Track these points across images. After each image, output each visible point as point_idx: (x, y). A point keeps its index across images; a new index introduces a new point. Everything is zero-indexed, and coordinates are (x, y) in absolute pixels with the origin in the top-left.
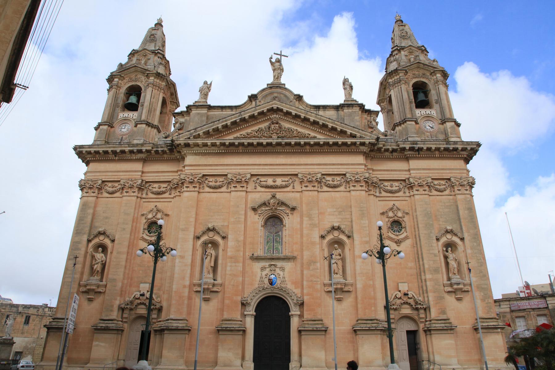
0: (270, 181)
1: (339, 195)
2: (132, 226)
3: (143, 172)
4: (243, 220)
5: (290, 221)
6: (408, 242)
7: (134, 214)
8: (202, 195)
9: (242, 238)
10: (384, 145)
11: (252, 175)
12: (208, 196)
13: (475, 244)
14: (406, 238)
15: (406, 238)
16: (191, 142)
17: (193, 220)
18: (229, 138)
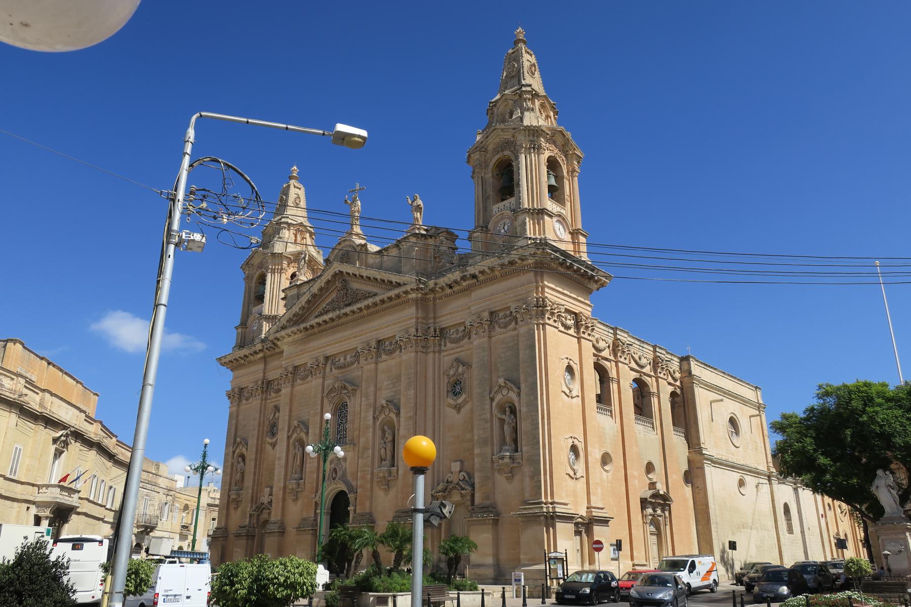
2: (259, 431)
3: (264, 373)
4: (319, 410)
6: (468, 407)
7: (260, 418)
9: (318, 432)
11: (327, 358)
12: (300, 387)
13: (532, 398)
14: (465, 402)
15: (465, 402)
16: (278, 335)
17: (287, 418)
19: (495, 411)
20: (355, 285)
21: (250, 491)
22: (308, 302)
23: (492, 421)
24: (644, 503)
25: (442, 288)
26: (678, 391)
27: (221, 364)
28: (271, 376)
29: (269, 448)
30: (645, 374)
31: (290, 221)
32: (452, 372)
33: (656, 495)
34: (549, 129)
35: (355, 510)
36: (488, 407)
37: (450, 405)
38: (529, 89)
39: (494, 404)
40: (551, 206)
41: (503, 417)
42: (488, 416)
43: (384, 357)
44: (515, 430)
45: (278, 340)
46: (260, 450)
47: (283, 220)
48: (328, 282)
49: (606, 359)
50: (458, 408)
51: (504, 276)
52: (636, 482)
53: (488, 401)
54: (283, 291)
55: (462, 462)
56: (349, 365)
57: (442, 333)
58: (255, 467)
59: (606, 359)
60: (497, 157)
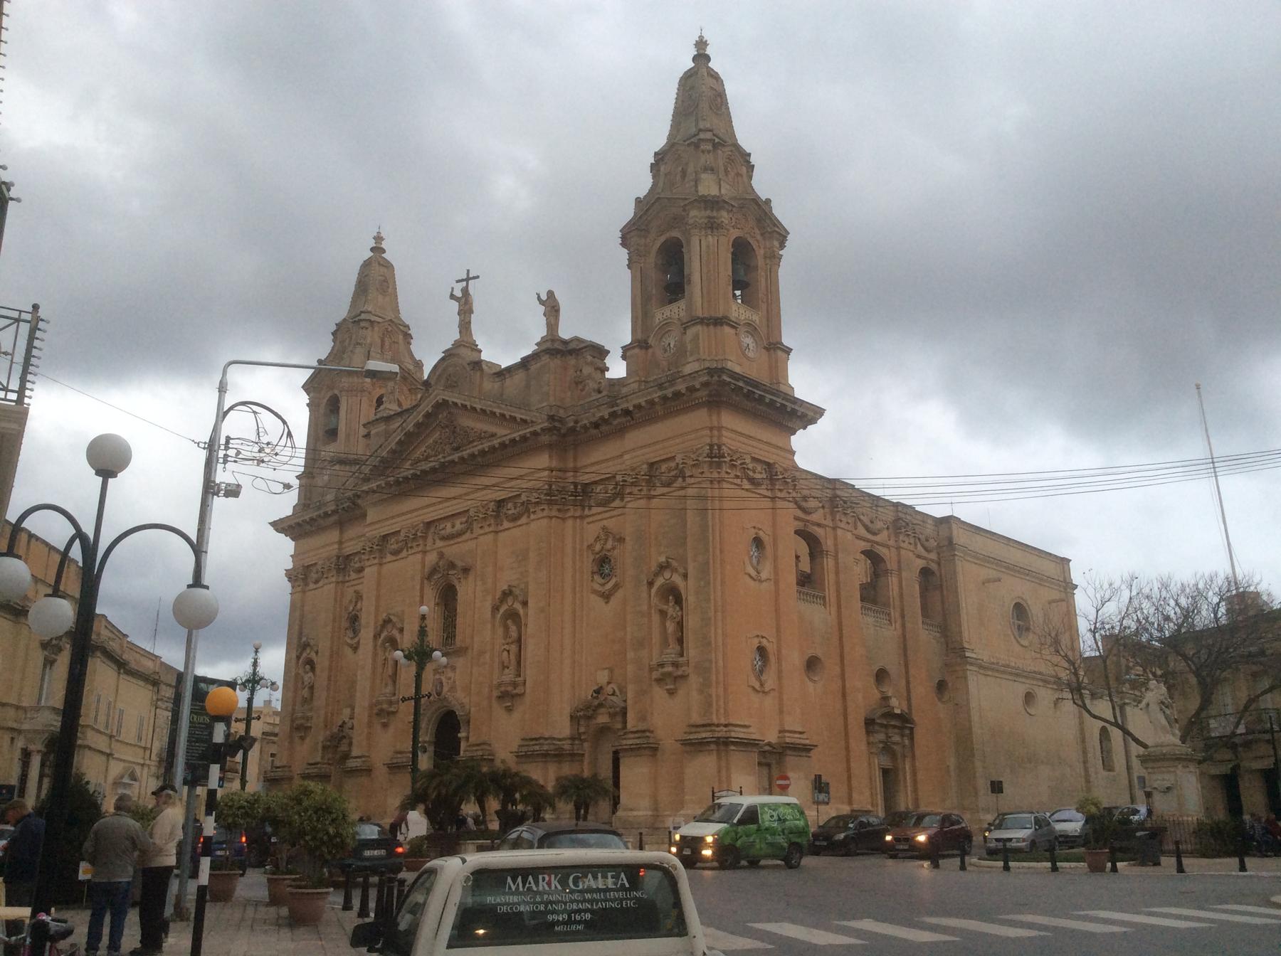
0: (449, 530)
1: (513, 535)
5: (465, 591)
6: (619, 594)
8: (385, 568)
10: (576, 422)
12: (393, 566)
14: (617, 587)
17: (373, 609)
18: (406, 470)
19: (655, 600)
20: (466, 422)
21: (322, 712)
22: (400, 443)
23: (650, 614)
24: (869, 723)
25: (585, 428)
26: (934, 566)
27: (277, 530)
28: (349, 548)
29: (348, 651)
30: (877, 543)
31: (373, 318)
32: (598, 547)
33: (890, 715)
34: (735, 199)
35: (467, 738)
36: (645, 595)
37: (594, 592)
38: (708, 135)
39: (654, 590)
40: (738, 311)
41: (665, 607)
42: (645, 608)
43: (506, 524)
44: (680, 625)
45: (359, 497)
46: (335, 655)
47: (363, 316)
48: (428, 415)
49: (819, 525)
50: (607, 597)
51: (669, 414)
52: (860, 696)
53: (645, 588)
54: (364, 425)
55: (611, 670)
56: (460, 534)
57: (583, 493)
58: (329, 680)
59: (819, 525)
60: (663, 239)
